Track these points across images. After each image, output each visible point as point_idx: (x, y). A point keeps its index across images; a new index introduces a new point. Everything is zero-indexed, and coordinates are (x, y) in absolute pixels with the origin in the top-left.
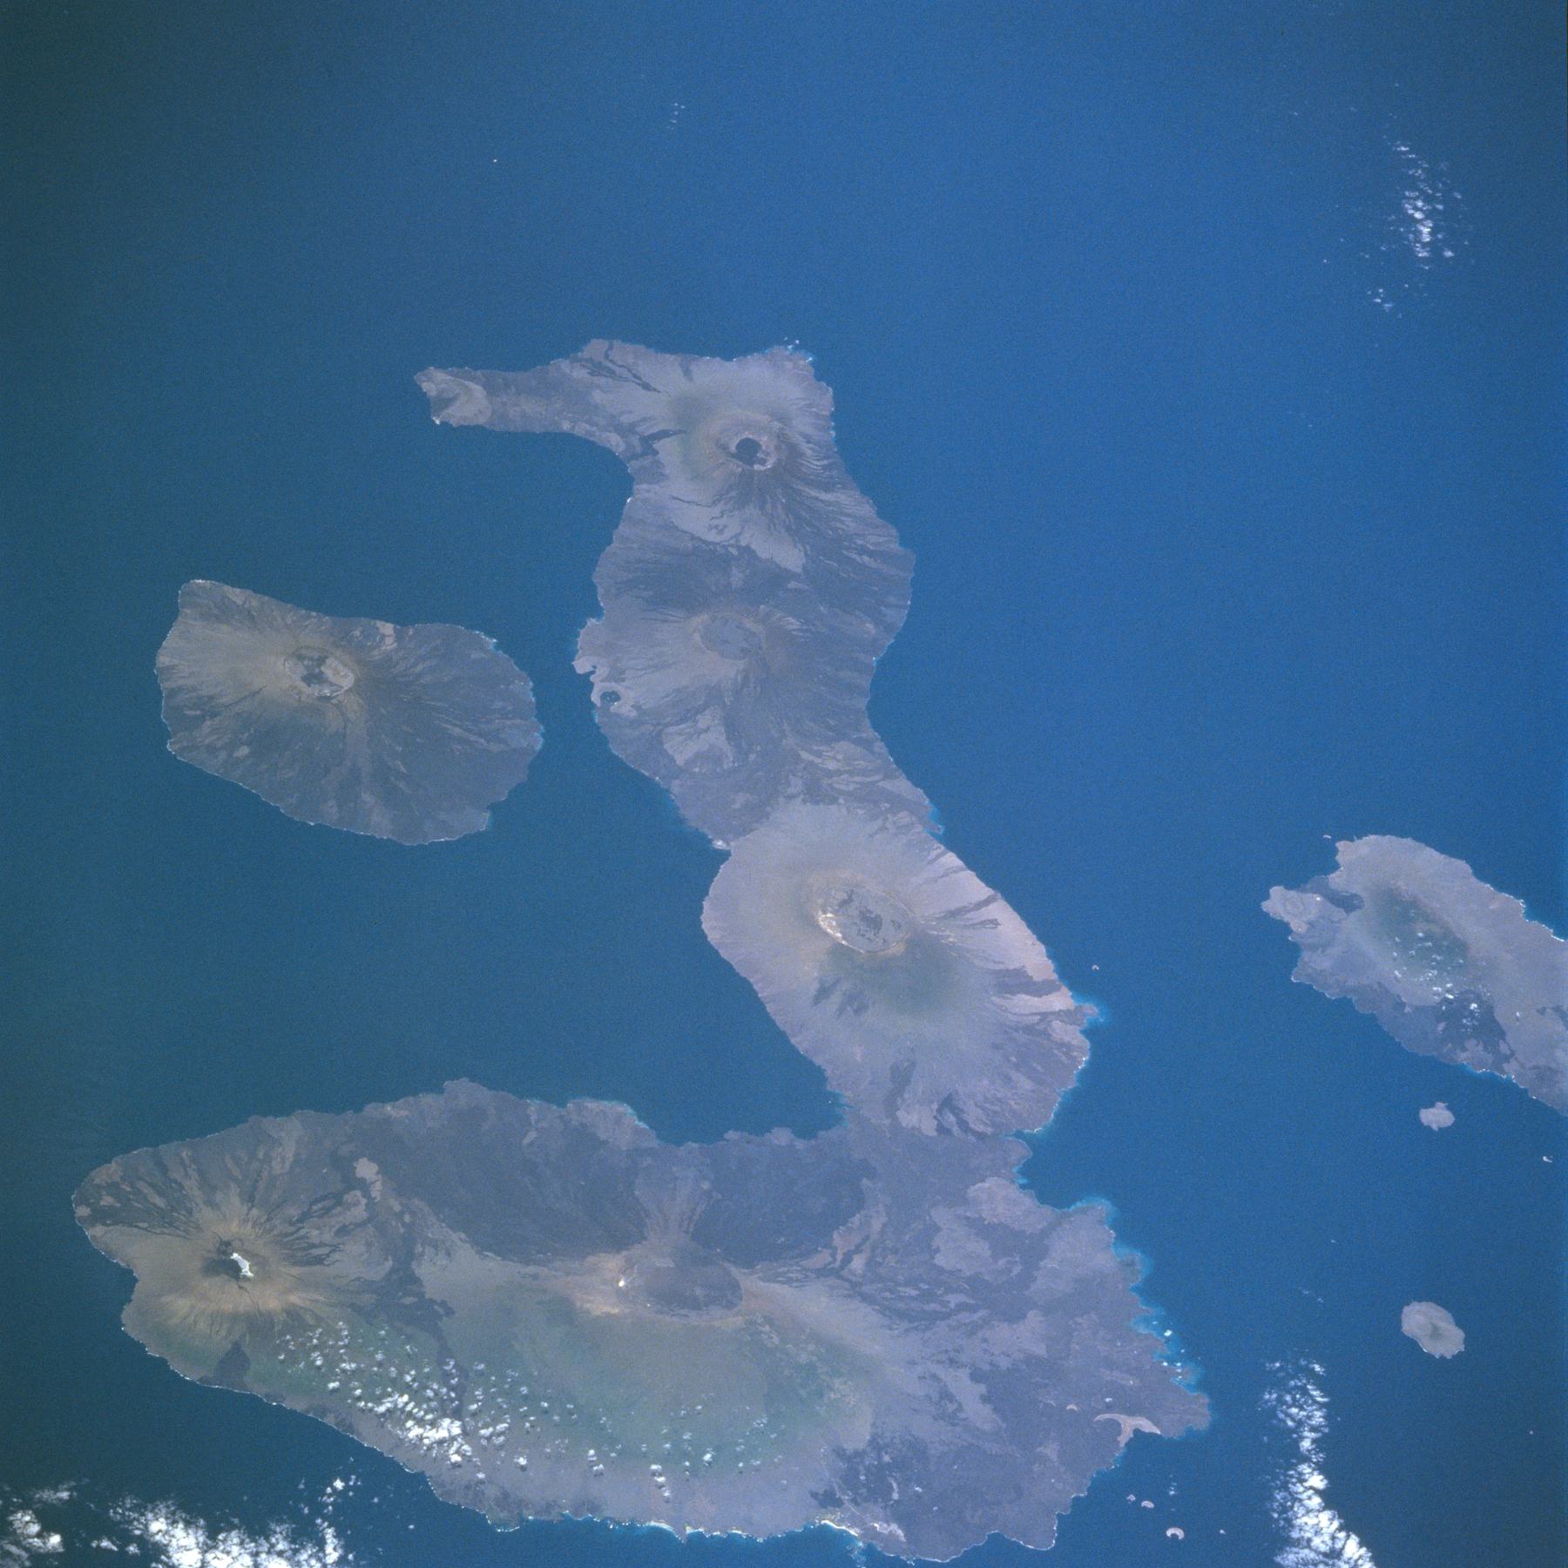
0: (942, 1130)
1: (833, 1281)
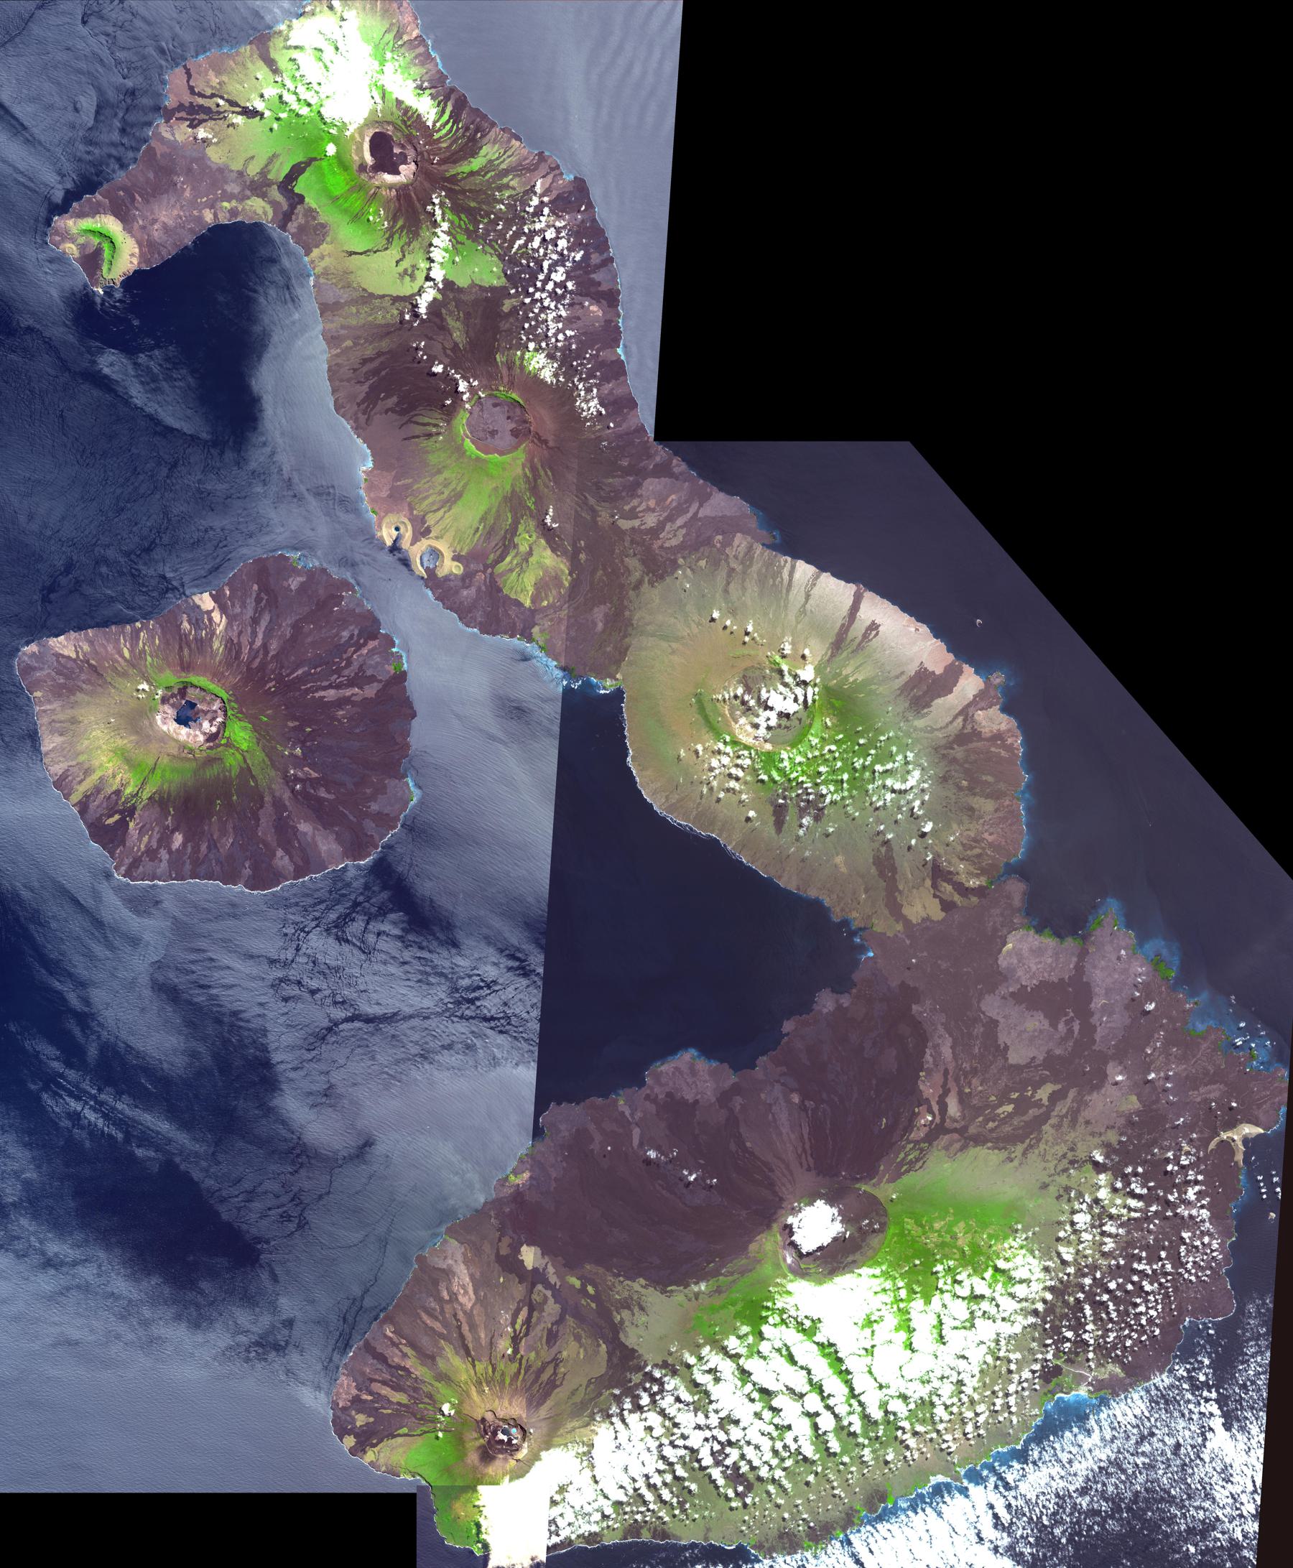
0: (947, 906)
1: (945, 1139)
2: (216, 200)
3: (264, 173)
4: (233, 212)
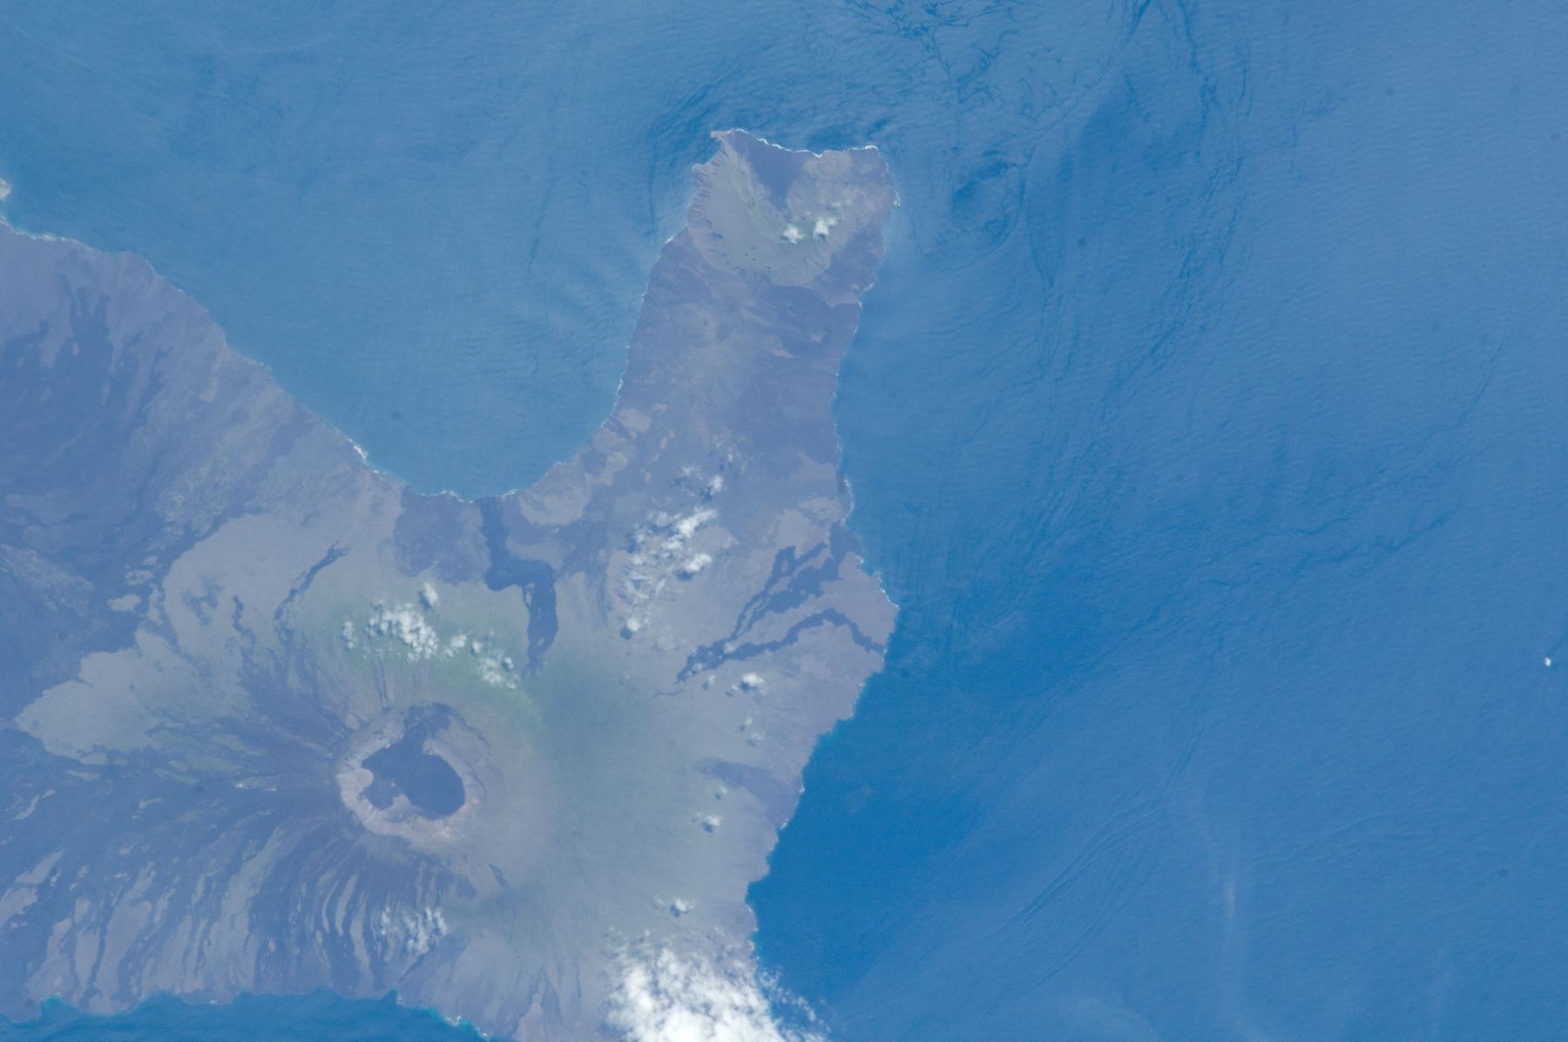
3: (596, 571)
4: (594, 461)
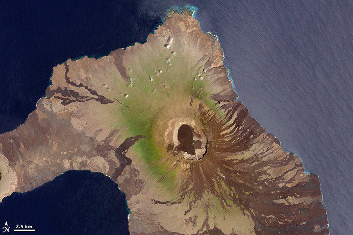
2: (72, 155)
3: (107, 141)
4: (83, 164)
